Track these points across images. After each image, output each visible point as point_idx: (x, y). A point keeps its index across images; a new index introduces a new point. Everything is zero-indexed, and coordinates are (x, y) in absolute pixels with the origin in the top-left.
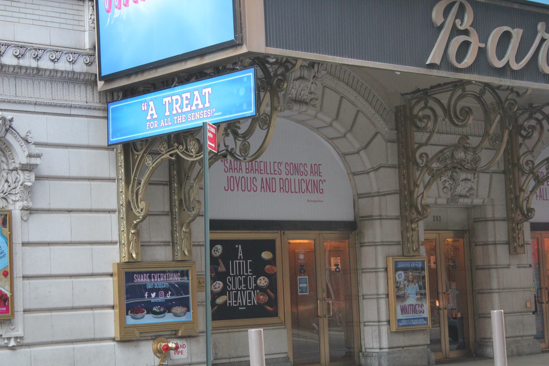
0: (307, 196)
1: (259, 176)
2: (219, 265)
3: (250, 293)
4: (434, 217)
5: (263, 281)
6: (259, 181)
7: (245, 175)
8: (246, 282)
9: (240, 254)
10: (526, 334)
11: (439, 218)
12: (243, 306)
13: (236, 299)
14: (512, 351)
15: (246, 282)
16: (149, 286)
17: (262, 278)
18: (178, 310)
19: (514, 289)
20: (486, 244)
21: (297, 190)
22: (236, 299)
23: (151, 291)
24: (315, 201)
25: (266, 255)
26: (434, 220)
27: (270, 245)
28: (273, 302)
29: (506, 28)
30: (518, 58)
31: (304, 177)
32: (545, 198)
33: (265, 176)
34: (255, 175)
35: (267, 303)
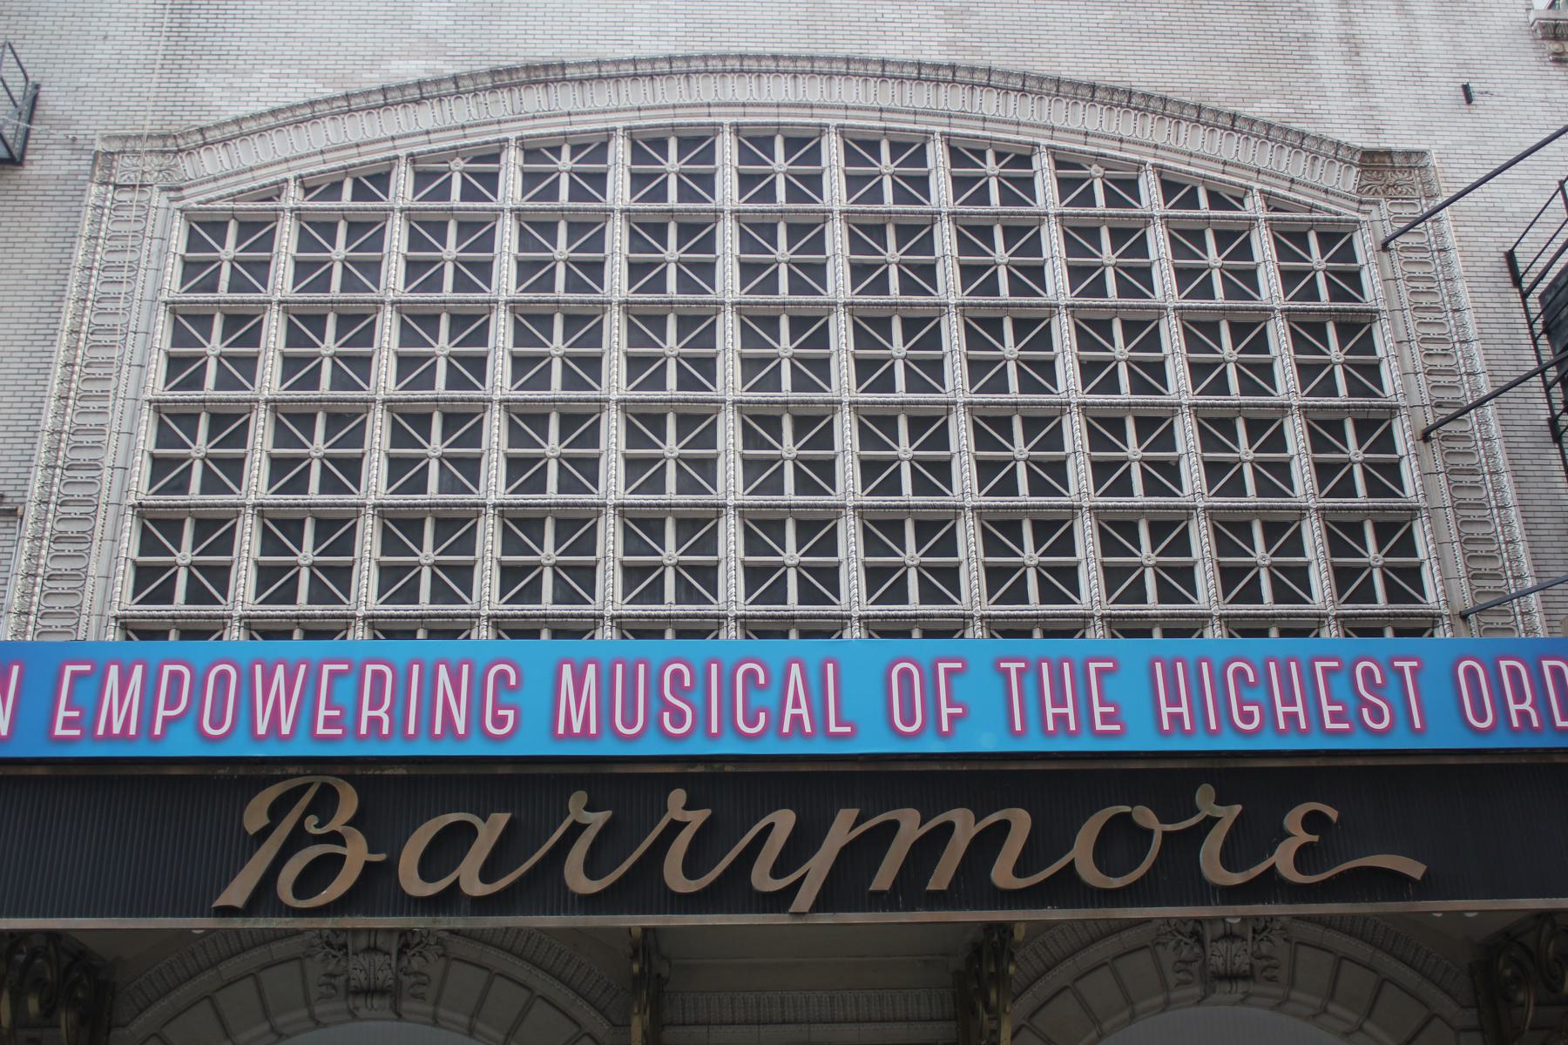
29: (453, 817)
30: (487, 874)
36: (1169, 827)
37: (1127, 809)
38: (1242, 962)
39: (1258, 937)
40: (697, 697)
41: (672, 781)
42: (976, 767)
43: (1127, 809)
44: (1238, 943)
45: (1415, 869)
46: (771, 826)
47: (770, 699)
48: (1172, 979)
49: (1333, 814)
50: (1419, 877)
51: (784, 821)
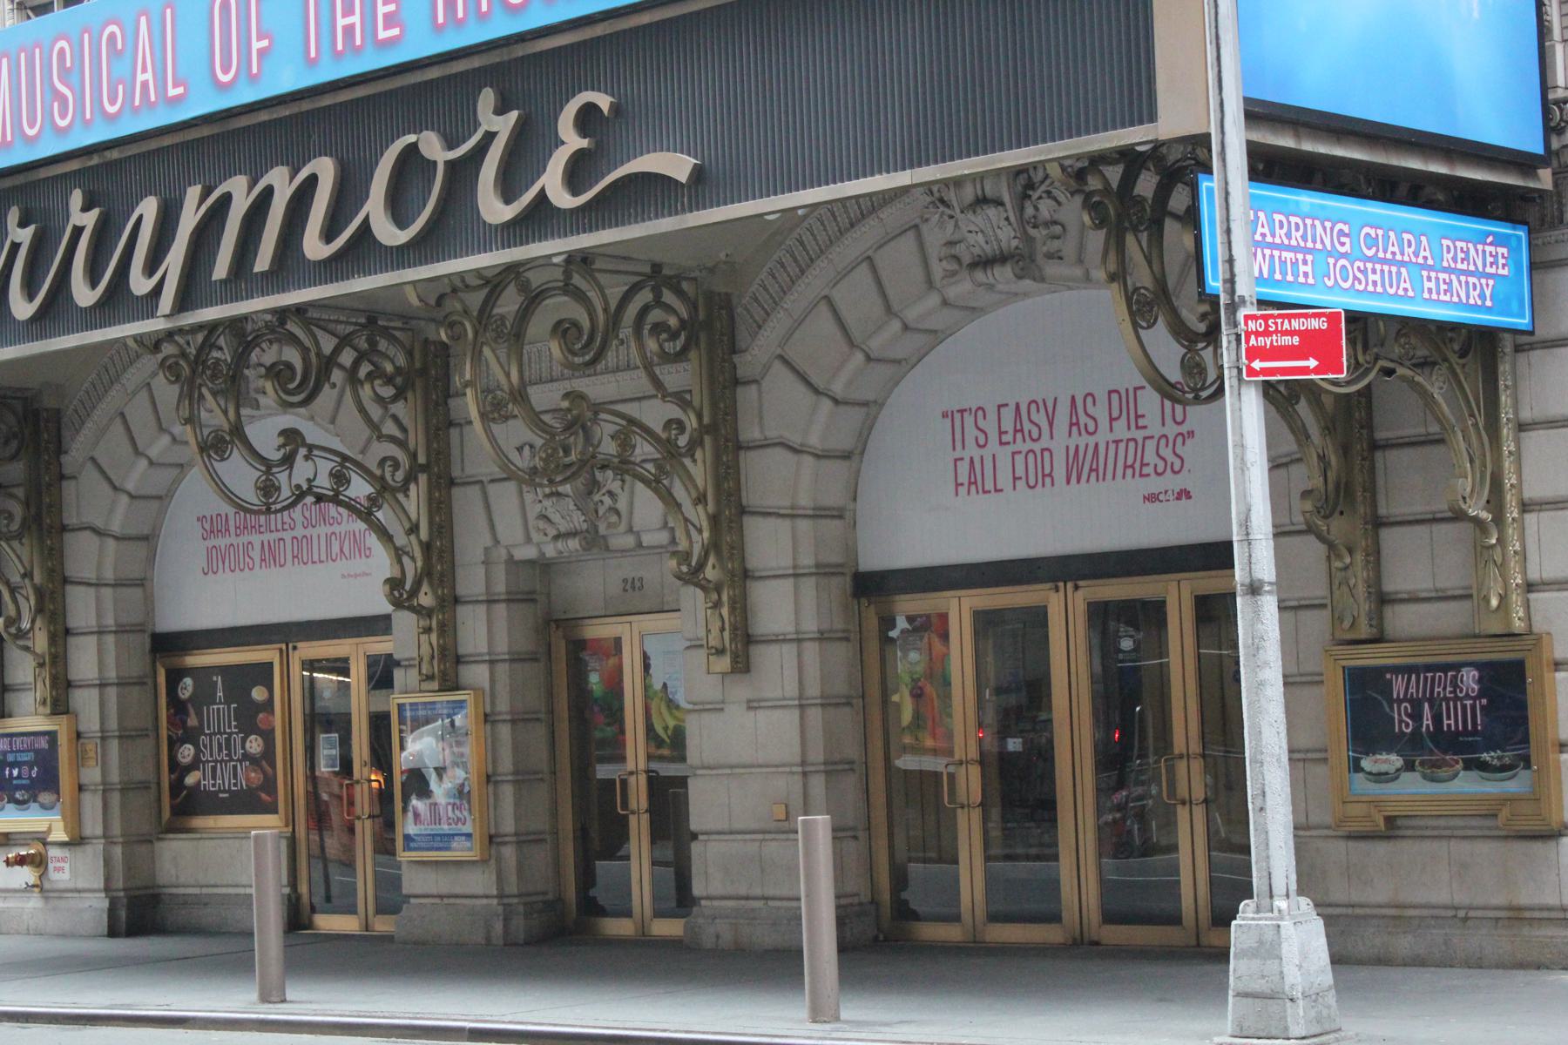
0: (342, 566)
1: (256, 539)
2: (188, 715)
3: (235, 767)
4: (625, 581)
5: (254, 745)
6: (258, 547)
7: (233, 540)
8: (229, 748)
9: (220, 694)
10: (771, 892)
11: (638, 584)
12: (224, 791)
13: (214, 778)
14: (718, 937)
15: (229, 748)
16: (10, 758)
17: (253, 737)
18: (45, 797)
19: (745, 767)
20: (823, 637)
21: (323, 557)
22: (214, 778)
23: (12, 765)
24: (356, 576)
25: (258, 694)
26: (625, 590)
27: (262, 673)
28: (269, 785)
31: (336, 528)
32: (989, 486)
33: (267, 537)
34: (250, 538)
35: (261, 788)
36: (453, 155)
37: (412, 138)
38: (1007, 237)
39: (1035, 195)
40: (75, 79)
41: (69, 180)
42: (293, 109)
43: (412, 138)
44: (992, 212)
45: (677, 165)
46: (141, 217)
47: (122, 69)
48: (938, 269)
49: (604, 101)
50: (682, 176)
51: (148, 209)
